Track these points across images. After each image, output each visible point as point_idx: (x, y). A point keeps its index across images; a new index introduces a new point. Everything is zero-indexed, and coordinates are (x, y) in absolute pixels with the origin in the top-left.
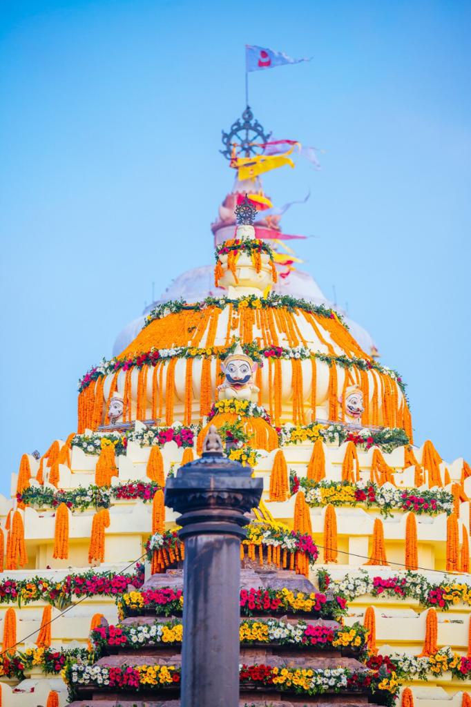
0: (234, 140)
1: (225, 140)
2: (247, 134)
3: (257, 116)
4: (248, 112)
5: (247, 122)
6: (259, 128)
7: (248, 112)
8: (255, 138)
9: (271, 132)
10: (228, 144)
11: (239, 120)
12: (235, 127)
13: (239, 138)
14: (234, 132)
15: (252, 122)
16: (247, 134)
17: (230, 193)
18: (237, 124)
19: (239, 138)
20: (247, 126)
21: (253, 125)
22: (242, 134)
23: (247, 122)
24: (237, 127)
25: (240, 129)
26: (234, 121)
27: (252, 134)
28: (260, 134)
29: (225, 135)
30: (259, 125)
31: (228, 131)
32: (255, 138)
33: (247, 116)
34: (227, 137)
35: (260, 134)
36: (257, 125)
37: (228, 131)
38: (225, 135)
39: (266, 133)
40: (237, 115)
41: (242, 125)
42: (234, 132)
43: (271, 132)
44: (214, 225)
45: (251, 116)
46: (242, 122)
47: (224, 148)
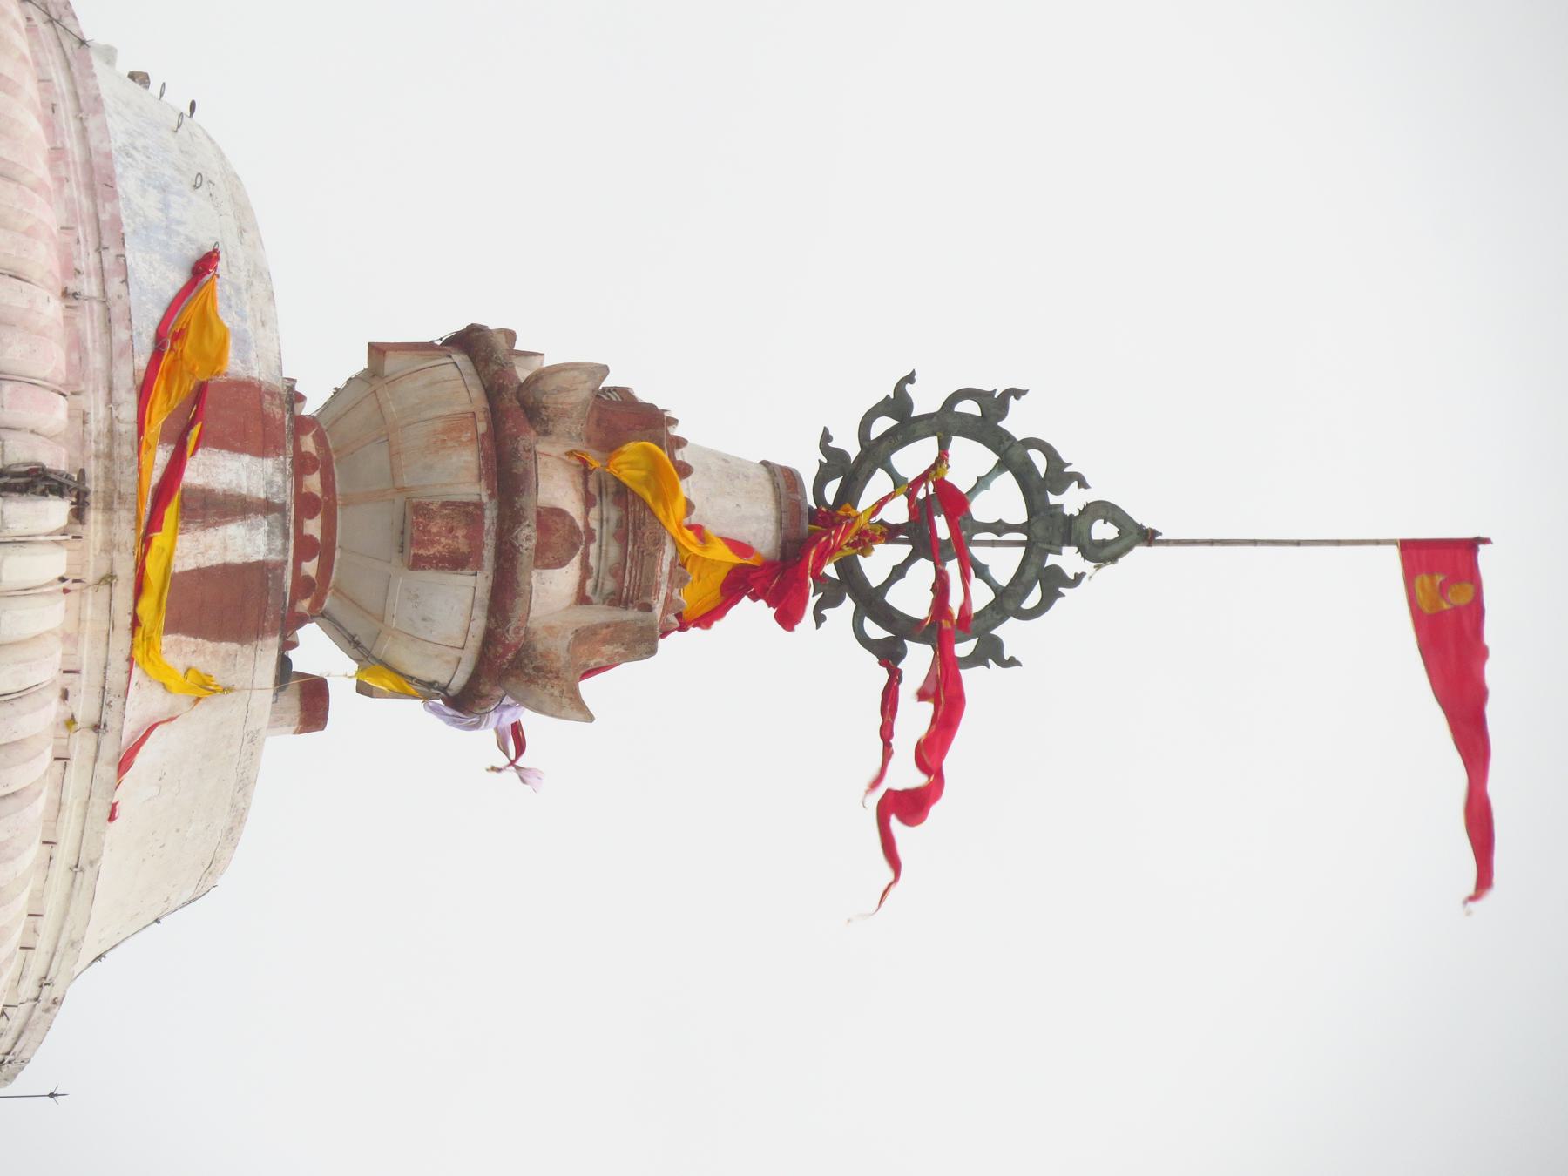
1: (969, 407)
4: (1149, 537)
5: (1069, 531)
7: (1149, 537)
9: (1012, 662)
10: (945, 424)
11: (1083, 484)
12: (1039, 460)
14: (1011, 455)
15: (1068, 560)
18: (1060, 476)
21: (1051, 560)
23: (1069, 531)
25: (1033, 488)
26: (1074, 460)
31: (1016, 423)
35: (1007, 602)
36: (1054, 583)
37: (1016, 423)
38: (995, 405)
39: (1010, 632)
41: (1053, 499)
42: (1011, 455)
43: (1012, 662)
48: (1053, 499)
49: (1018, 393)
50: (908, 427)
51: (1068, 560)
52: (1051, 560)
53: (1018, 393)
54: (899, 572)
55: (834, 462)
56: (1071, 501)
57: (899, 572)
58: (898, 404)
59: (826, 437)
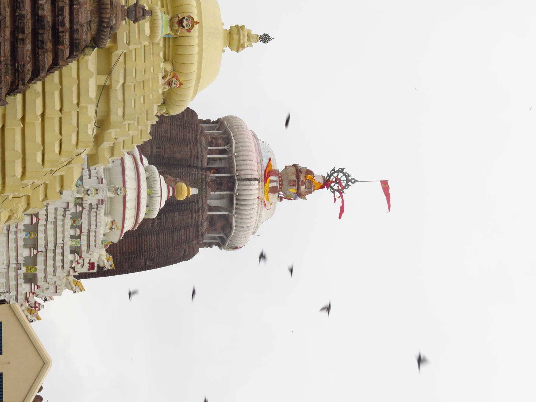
0: (340, 175)
1: (340, 170)
3: (353, 187)
5: (350, 181)
6: (347, 187)
9: (345, 193)
10: (338, 171)
11: (351, 176)
13: (342, 177)
14: (344, 174)
15: (350, 183)
17: (314, 173)
18: (349, 176)
19: (342, 177)
20: (348, 181)
21: (348, 184)
22: (344, 178)
23: (350, 181)
24: (347, 176)
25: (346, 177)
26: (350, 174)
29: (343, 169)
31: (345, 171)
33: (353, 181)
34: (342, 171)
36: (349, 186)
37: (345, 171)
38: (343, 169)
39: (345, 190)
40: (353, 176)
41: (348, 178)
42: (344, 174)
43: (345, 193)
44: (297, 165)
45: (353, 183)
46: (350, 178)
47: (336, 169)
48: (348, 178)
49: (345, 168)
50: (335, 172)
51: (350, 183)
52: (348, 184)
53: (345, 168)
54: (334, 185)
55: (328, 175)
56: (350, 178)
57: (334, 185)
58: (334, 170)
59: (327, 173)
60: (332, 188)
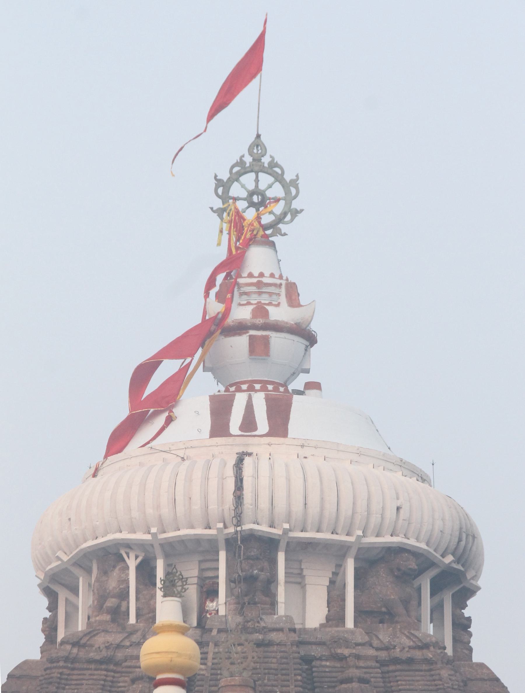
0: (236, 190)
1: (220, 191)
2: (257, 180)
5: (257, 160)
8: (270, 186)
9: (297, 176)
10: (225, 197)
11: (243, 156)
13: (243, 186)
14: (235, 178)
15: (266, 160)
16: (257, 180)
18: (241, 163)
19: (243, 186)
21: (266, 165)
22: (248, 180)
23: (257, 160)
25: (245, 171)
26: (236, 158)
27: (265, 179)
28: (279, 178)
29: (219, 182)
30: (277, 165)
31: (225, 176)
32: (270, 186)
35: (279, 178)
36: (273, 164)
37: (225, 176)
38: (219, 182)
39: (288, 177)
41: (248, 165)
42: (235, 178)
43: (297, 176)
46: (248, 159)
48: (248, 165)
49: (216, 176)
51: (266, 160)
52: (266, 165)
53: (216, 176)
56: (248, 159)
60: (280, 219)
